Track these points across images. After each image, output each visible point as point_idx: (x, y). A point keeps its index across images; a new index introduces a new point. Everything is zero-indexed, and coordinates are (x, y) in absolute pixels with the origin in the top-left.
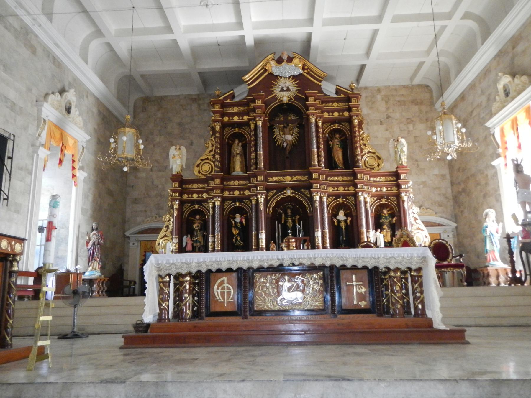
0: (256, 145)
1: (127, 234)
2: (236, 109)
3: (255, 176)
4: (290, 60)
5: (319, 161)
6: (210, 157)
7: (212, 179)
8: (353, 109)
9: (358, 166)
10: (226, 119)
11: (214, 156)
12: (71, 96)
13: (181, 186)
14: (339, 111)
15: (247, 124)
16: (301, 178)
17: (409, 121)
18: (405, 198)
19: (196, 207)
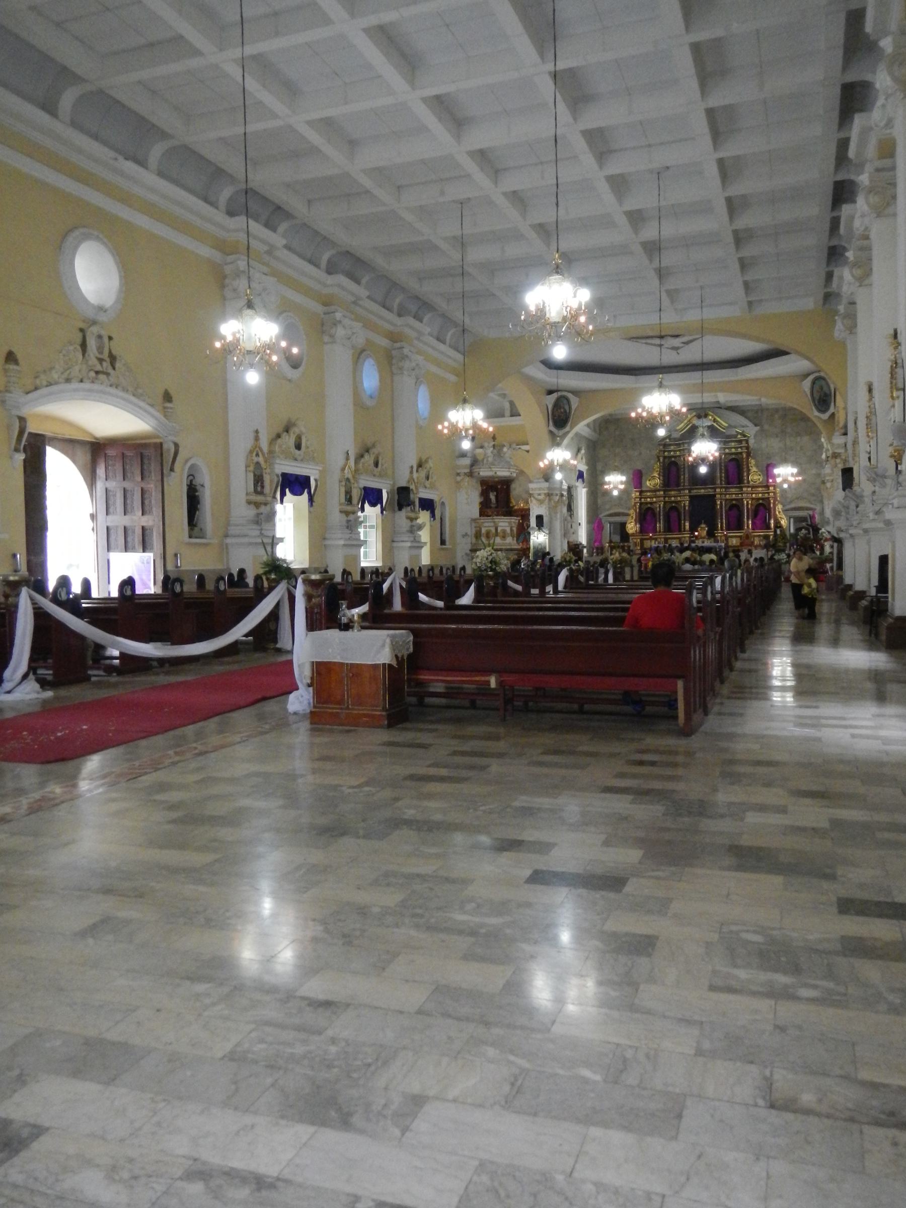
0: (684, 471)
1: (601, 516)
2: (672, 448)
3: (684, 489)
4: (706, 416)
5: (721, 480)
6: (657, 476)
7: (659, 490)
8: (744, 448)
9: (743, 483)
10: (666, 454)
11: (659, 474)
12: (583, 451)
13: (640, 495)
14: (734, 448)
15: (679, 456)
16: (710, 490)
17: (798, 434)
18: (772, 501)
19: (649, 505)
